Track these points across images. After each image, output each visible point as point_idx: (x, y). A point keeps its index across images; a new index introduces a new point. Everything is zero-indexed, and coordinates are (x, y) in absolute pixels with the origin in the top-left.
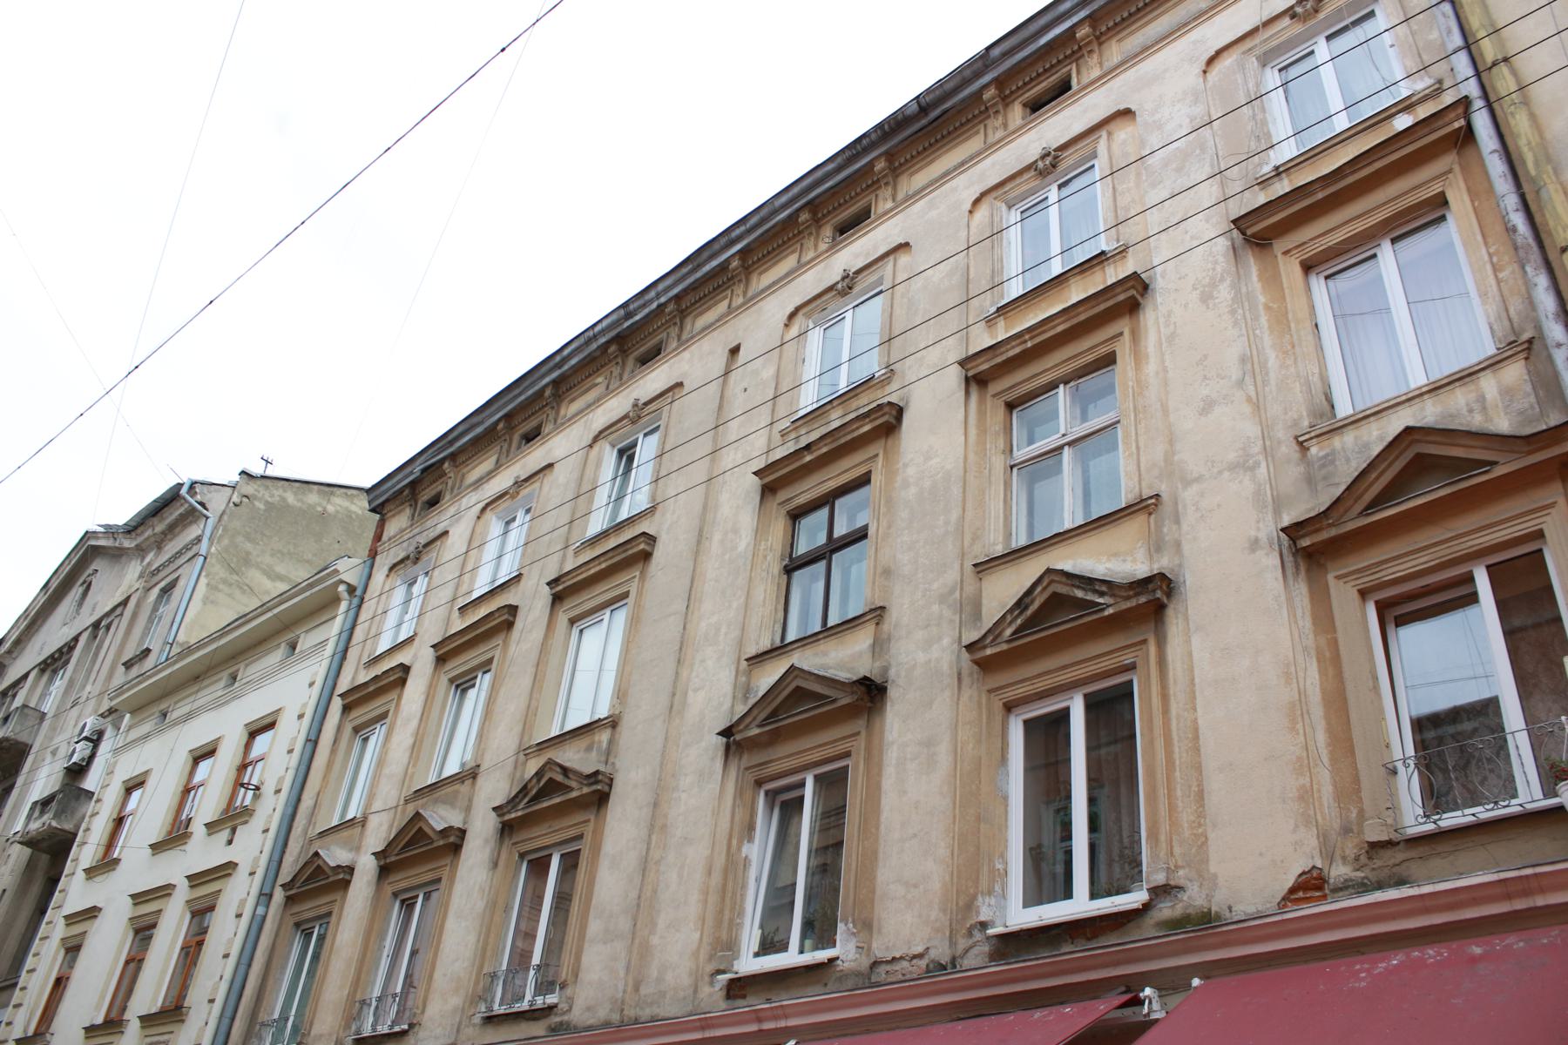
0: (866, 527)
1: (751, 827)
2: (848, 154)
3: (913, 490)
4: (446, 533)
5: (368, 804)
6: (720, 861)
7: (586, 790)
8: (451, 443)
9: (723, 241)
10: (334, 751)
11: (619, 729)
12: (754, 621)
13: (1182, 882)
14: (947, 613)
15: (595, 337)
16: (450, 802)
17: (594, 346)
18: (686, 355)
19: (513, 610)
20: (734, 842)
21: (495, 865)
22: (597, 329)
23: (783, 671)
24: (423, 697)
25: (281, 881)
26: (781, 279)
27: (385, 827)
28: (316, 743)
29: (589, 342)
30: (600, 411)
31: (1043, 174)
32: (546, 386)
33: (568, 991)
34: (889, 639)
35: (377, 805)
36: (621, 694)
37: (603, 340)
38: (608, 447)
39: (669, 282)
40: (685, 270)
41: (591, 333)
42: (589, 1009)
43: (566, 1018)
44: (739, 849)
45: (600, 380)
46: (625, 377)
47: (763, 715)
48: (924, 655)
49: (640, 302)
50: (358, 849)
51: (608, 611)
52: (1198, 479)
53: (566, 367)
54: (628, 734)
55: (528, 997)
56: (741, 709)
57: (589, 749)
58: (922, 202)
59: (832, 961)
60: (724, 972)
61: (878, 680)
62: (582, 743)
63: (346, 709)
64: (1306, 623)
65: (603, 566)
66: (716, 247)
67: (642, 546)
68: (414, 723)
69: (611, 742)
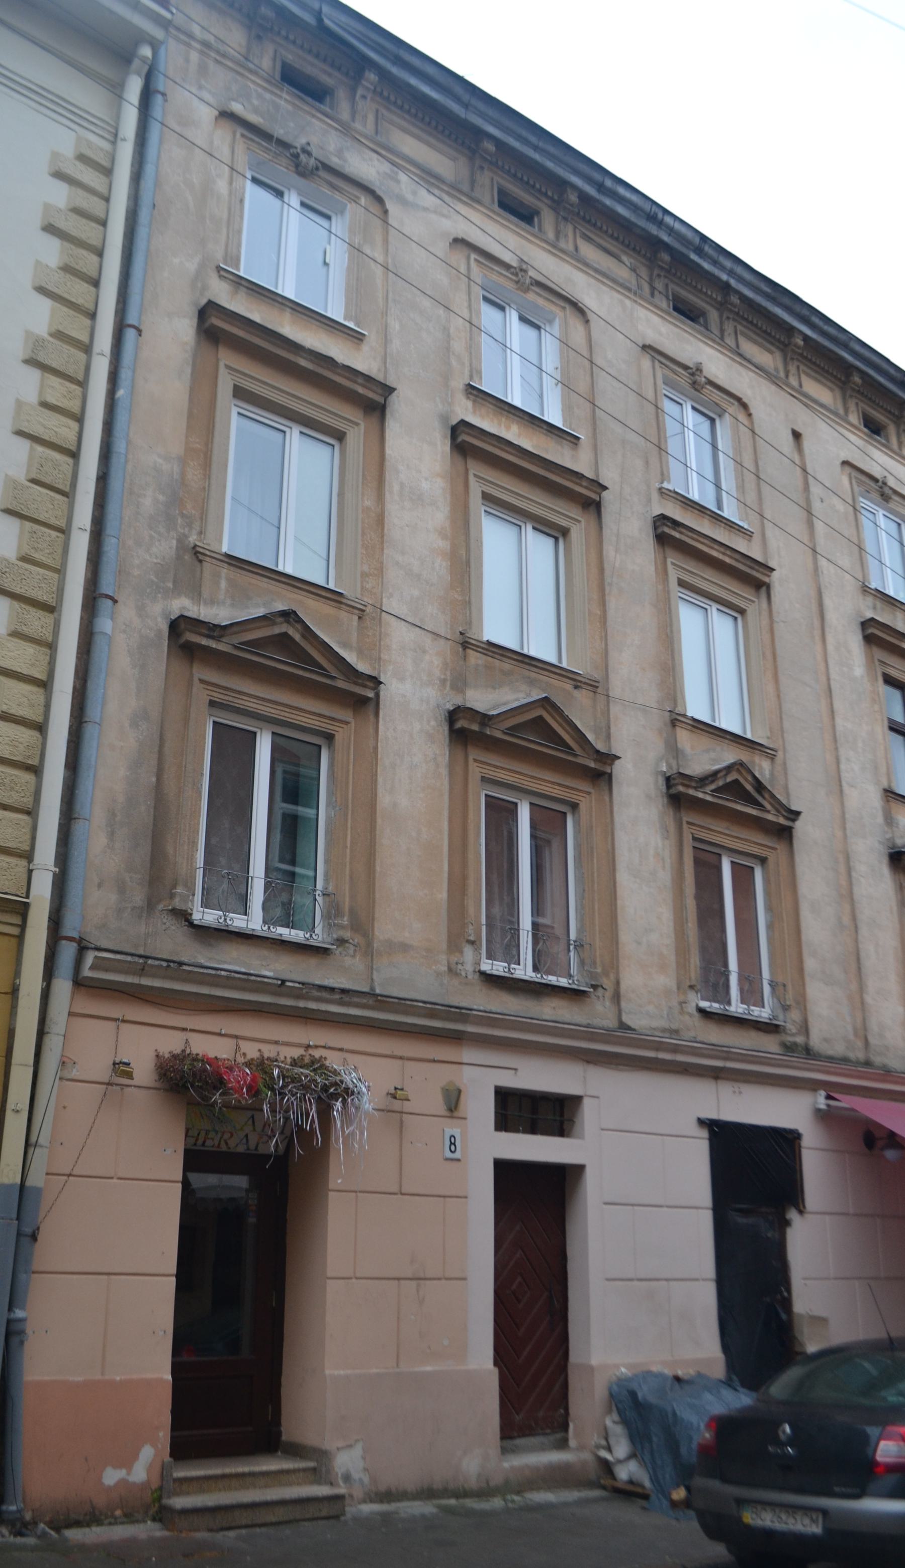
9: (805, 312)
15: (660, 224)
17: (653, 230)
39: (747, 276)
53: (608, 202)
65: (727, 560)
66: (797, 308)
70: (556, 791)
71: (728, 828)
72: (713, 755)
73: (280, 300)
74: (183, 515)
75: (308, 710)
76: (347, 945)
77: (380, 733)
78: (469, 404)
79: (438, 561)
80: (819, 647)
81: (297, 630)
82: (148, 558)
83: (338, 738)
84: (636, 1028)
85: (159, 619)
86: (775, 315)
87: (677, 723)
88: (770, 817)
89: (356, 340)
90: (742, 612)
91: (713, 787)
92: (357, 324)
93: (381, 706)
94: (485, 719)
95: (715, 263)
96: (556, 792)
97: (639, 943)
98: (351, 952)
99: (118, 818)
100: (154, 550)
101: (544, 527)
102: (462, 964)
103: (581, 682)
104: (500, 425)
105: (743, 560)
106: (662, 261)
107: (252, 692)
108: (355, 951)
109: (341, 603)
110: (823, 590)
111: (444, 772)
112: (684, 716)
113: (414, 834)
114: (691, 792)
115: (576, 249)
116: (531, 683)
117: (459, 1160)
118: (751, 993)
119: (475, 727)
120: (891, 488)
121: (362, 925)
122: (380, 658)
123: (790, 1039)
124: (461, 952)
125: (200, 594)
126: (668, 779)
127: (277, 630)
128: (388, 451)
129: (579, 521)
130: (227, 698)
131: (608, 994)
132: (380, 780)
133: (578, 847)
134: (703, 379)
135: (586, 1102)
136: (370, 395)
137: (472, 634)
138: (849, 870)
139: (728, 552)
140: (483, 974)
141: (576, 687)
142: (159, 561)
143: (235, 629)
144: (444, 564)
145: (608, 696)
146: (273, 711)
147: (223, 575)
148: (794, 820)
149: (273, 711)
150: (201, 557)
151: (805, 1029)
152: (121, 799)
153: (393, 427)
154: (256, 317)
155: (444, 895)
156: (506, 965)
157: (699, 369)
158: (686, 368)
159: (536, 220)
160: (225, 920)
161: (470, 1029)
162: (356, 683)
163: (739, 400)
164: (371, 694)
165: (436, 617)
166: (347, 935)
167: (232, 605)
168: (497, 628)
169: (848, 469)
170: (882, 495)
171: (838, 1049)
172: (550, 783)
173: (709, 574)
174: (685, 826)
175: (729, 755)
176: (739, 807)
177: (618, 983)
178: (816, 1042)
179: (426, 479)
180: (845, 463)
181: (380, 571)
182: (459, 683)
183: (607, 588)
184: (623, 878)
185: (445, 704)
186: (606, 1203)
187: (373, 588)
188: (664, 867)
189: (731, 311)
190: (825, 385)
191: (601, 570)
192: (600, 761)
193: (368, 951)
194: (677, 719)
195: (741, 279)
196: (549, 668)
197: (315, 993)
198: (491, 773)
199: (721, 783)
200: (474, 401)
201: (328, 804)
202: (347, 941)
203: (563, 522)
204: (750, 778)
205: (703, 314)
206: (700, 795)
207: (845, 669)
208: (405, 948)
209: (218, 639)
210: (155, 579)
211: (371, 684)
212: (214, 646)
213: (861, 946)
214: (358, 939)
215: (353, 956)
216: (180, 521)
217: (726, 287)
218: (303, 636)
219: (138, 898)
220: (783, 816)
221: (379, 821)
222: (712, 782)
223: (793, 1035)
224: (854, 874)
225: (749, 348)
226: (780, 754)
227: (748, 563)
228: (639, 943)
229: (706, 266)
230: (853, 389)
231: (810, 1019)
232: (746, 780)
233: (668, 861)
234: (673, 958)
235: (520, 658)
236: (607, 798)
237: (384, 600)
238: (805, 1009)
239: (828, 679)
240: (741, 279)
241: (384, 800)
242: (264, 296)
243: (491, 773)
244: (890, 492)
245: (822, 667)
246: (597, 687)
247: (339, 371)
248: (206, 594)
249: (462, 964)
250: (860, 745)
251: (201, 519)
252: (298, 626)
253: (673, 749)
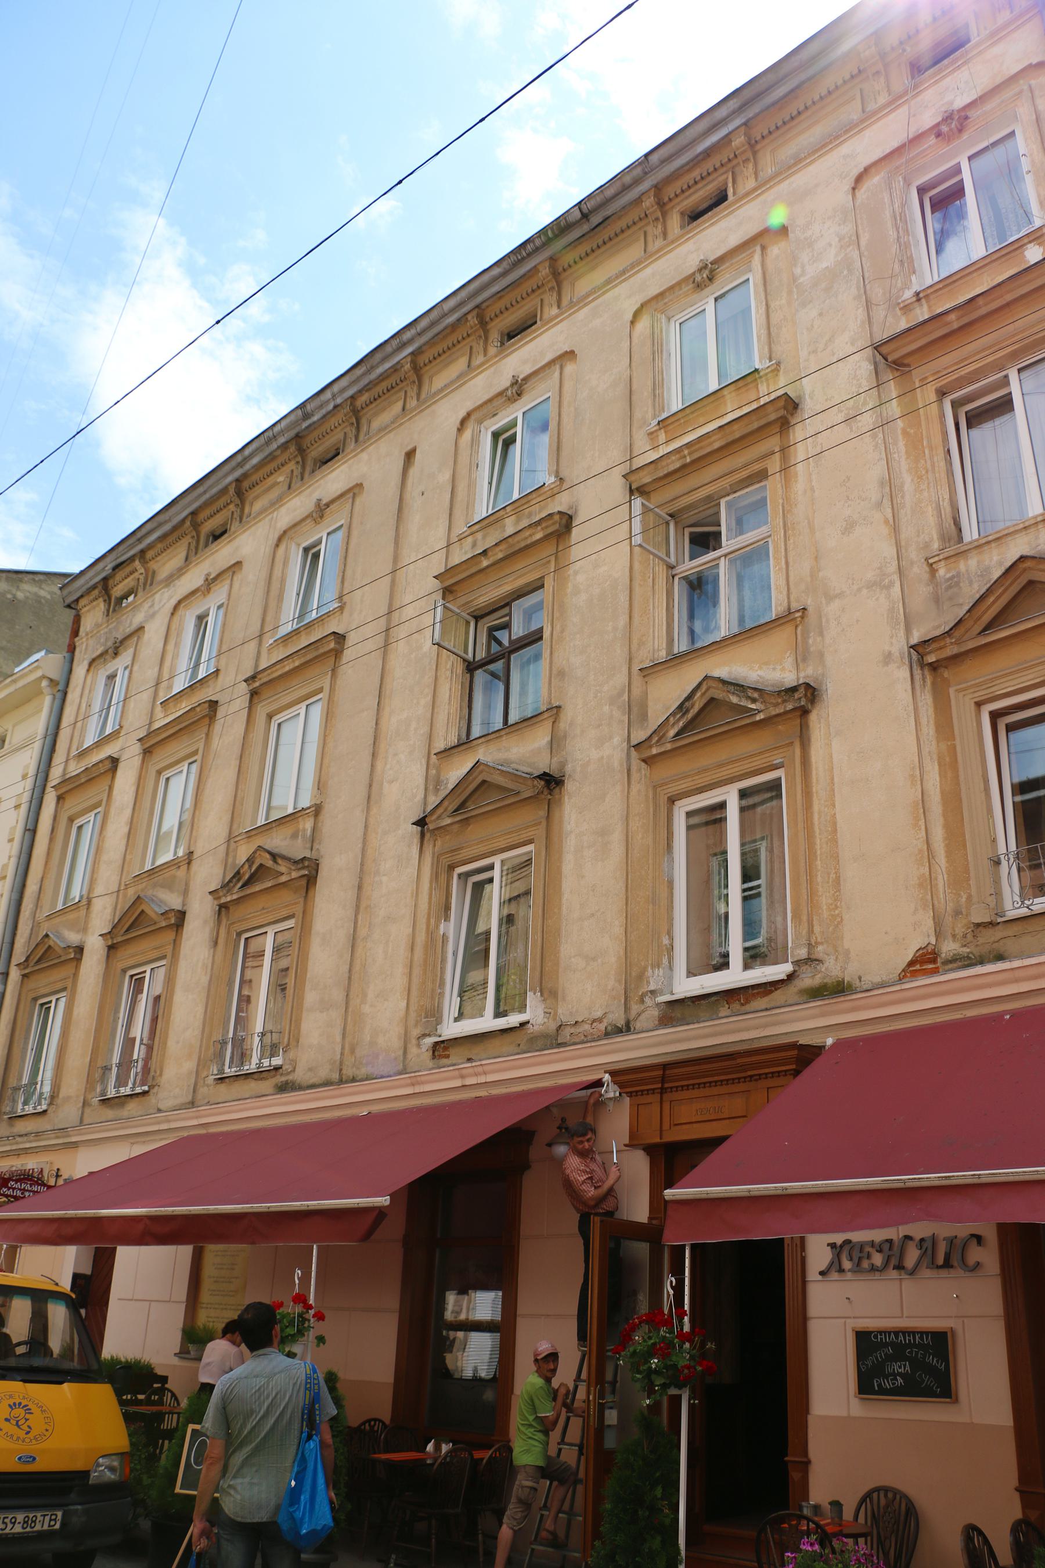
0: (541, 630)
1: (447, 908)
2: (513, 258)
3: (584, 597)
4: (141, 629)
5: (90, 890)
6: (421, 938)
7: (294, 875)
8: (140, 540)
9: (395, 343)
10: (52, 839)
11: (321, 817)
12: (442, 718)
13: (821, 956)
14: (617, 714)
16: (169, 886)
18: (364, 456)
19: (213, 705)
20: (432, 921)
21: (216, 943)
22: (277, 429)
23: (470, 765)
24: (134, 788)
25: (15, 961)
26: (452, 382)
27: (109, 910)
28: (34, 831)
29: (268, 443)
30: (283, 510)
31: (699, 287)
32: (230, 484)
33: (291, 1054)
34: (565, 737)
35: (99, 890)
36: (320, 785)
37: (282, 440)
38: (293, 547)
39: (344, 382)
40: (358, 372)
41: (270, 434)
42: (310, 1070)
43: (290, 1077)
44: (437, 927)
45: (281, 479)
46: (306, 475)
47: (452, 808)
48: (596, 750)
49: (316, 402)
50: (85, 930)
51: (303, 705)
52: (841, 595)
54: (329, 823)
55: (255, 1060)
56: (433, 801)
57: (295, 836)
58: (585, 310)
59: (523, 1025)
60: (429, 1035)
61: (556, 774)
62: (287, 830)
63: (60, 798)
64: (929, 730)
67: (332, 645)
68: (128, 812)
69: (314, 829)
95: (321, 407)
222: (239, 880)
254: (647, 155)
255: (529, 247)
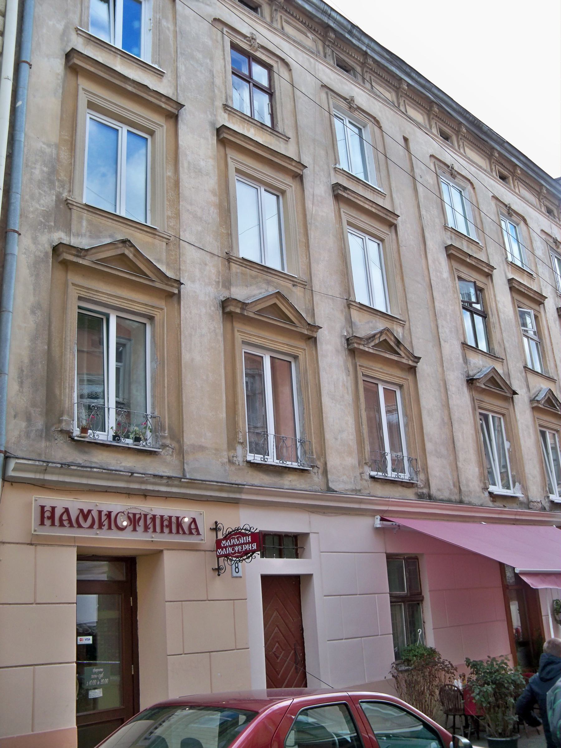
2: (461, 110)
9: (408, 70)
15: (329, 16)
17: (326, 19)
29: (324, 12)
39: (377, 48)
65: (374, 210)
66: (404, 67)
70: (285, 349)
71: (381, 368)
72: (371, 325)
73: (114, 50)
74: (59, 180)
75: (139, 301)
76: (168, 448)
77: (182, 316)
78: (226, 116)
79: (212, 209)
80: (424, 261)
81: (131, 251)
82: (38, 206)
83: (157, 318)
84: (337, 490)
85: (46, 246)
86: (392, 71)
87: (351, 306)
88: (404, 361)
89: (159, 76)
90: (382, 240)
91: (373, 344)
92: (160, 66)
93: (182, 299)
94: (244, 305)
95: (359, 40)
96: (285, 349)
97: (336, 439)
98: (171, 453)
99: (25, 373)
100: (42, 202)
101: (272, 189)
102: (236, 457)
103: (296, 282)
104: (244, 128)
105: (382, 210)
106: (330, 38)
107: (105, 291)
108: (173, 452)
109: (156, 235)
110: (424, 228)
111: (221, 338)
112: (355, 302)
113: (204, 378)
114: (361, 347)
115: (283, 28)
116: (269, 283)
117: (241, 577)
118: (398, 466)
119: (238, 311)
120: (456, 171)
121: (177, 436)
122: (180, 269)
123: (420, 491)
124: (235, 450)
125: (70, 230)
126: (348, 340)
127: (119, 252)
128: (180, 143)
129: (291, 186)
130: (88, 295)
131: (320, 471)
132: (183, 344)
133: (299, 382)
134: (355, 106)
135: (311, 536)
136: (169, 108)
137: (234, 254)
138: (446, 390)
139: (374, 206)
140: (249, 462)
141: (294, 285)
142: (45, 209)
143: (93, 251)
144: (215, 211)
145: (312, 290)
146: (117, 302)
147: (84, 217)
148: (417, 363)
149: (117, 302)
150: (71, 206)
151: (428, 484)
152: (26, 360)
153: (182, 128)
154: (100, 60)
155: (224, 415)
156: (262, 456)
157: (352, 100)
158: (345, 99)
159: (259, 10)
160: (94, 436)
161: (244, 496)
162: (167, 284)
163: (374, 118)
164: (176, 291)
165: (213, 244)
166: (168, 442)
167: (91, 237)
168: (247, 249)
169: (433, 160)
170: (452, 175)
171: (446, 495)
172: (281, 343)
173: (364, 218)
174: (358, 368)
175: (381, 325)
176: (387, 356)
177: (326, 464)
178: (434, 491)
179: (203, 160)
180: (432, 156)
181: (177, 215)
182: (227, 284)
183: (309, 226)
184: (326, 400)
185: (219, 297)
186: (325, 596)
187: (174, 225)
188: (348, 393)
189: (368, 67)
190: (418, 112)
191: (305, 215)
192: (311, 330)
193: (181, 452)
194: (350, 303)
195: (373, 50)
196: (278, 274)
197: (152, 480)
198: (248, 338)
199: (377, 341)
200: (229, 114)
201: (152, 360)
202: (168, 446)
203: (283, 187)
204: (393, 338)
205: (353, 69)
206: (367, 349)
207: (438, 274)
208: (202, 448)
209: (83, 257)
210: (43, 221)
211: (176, 285)
212: (81, 262)
213: (454, 434)
214: (174, 444)
215: (172, 455)
216: (57, 184)
217: (366, 53)
218: (134, 255)
219: (40, 424)
220: (411, 360)
221: (183, 370)
223: (422, 488)
224: (449, 393)
225: (379, 89)
226: (407, 323)
227: (385, 212)
228: (336, 439)
229: (354, 41)
230: (434, 114)
231: (430, 478)
232: (391, 339)
233: (350, 389)
234: (355, 447)
235: (261, 268)
236: (314, 352)
237: (181, 233)
238: (427, 473)
239: (430, 280)
240: (373, 50)
241: (186, 357)
242: (105, 47)
243: (248, 338)
244: (456, 173)
245: (426, 273)
246: (306, 285)
247: (151, 94)
248: (74, 229)
249: (236, 457)
250: (448, 317)
251: (70, 183)
252: (132, 249)
253: (350, 322)
254: (507, 142)
255: (468, 116)
